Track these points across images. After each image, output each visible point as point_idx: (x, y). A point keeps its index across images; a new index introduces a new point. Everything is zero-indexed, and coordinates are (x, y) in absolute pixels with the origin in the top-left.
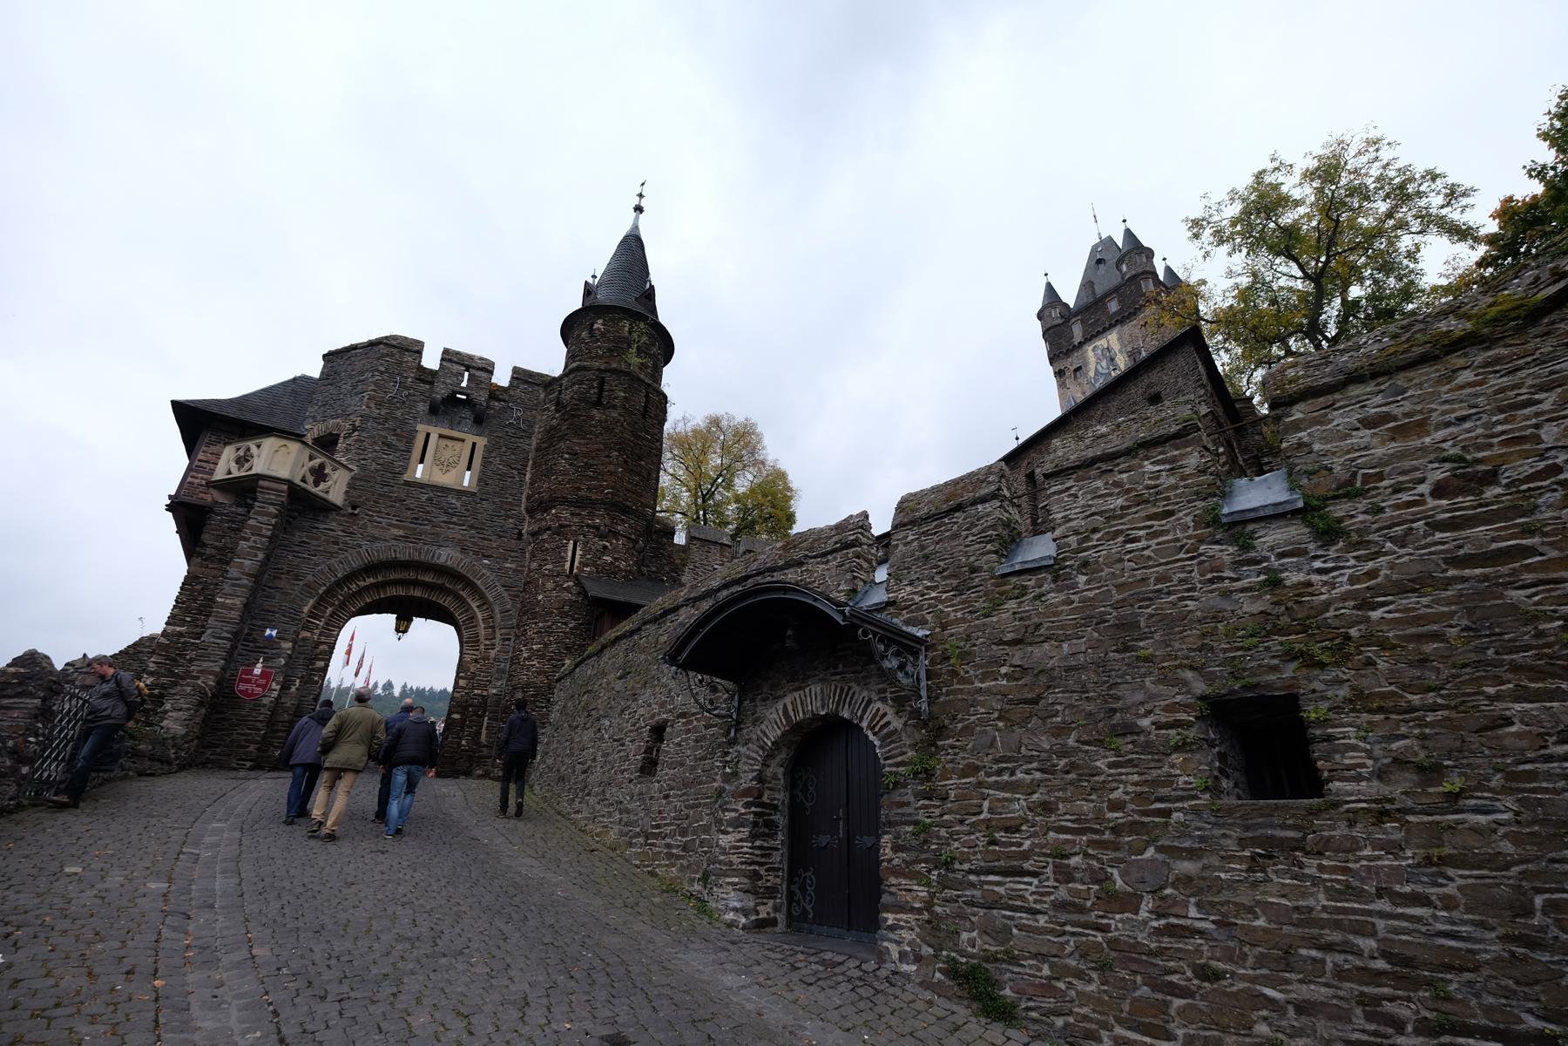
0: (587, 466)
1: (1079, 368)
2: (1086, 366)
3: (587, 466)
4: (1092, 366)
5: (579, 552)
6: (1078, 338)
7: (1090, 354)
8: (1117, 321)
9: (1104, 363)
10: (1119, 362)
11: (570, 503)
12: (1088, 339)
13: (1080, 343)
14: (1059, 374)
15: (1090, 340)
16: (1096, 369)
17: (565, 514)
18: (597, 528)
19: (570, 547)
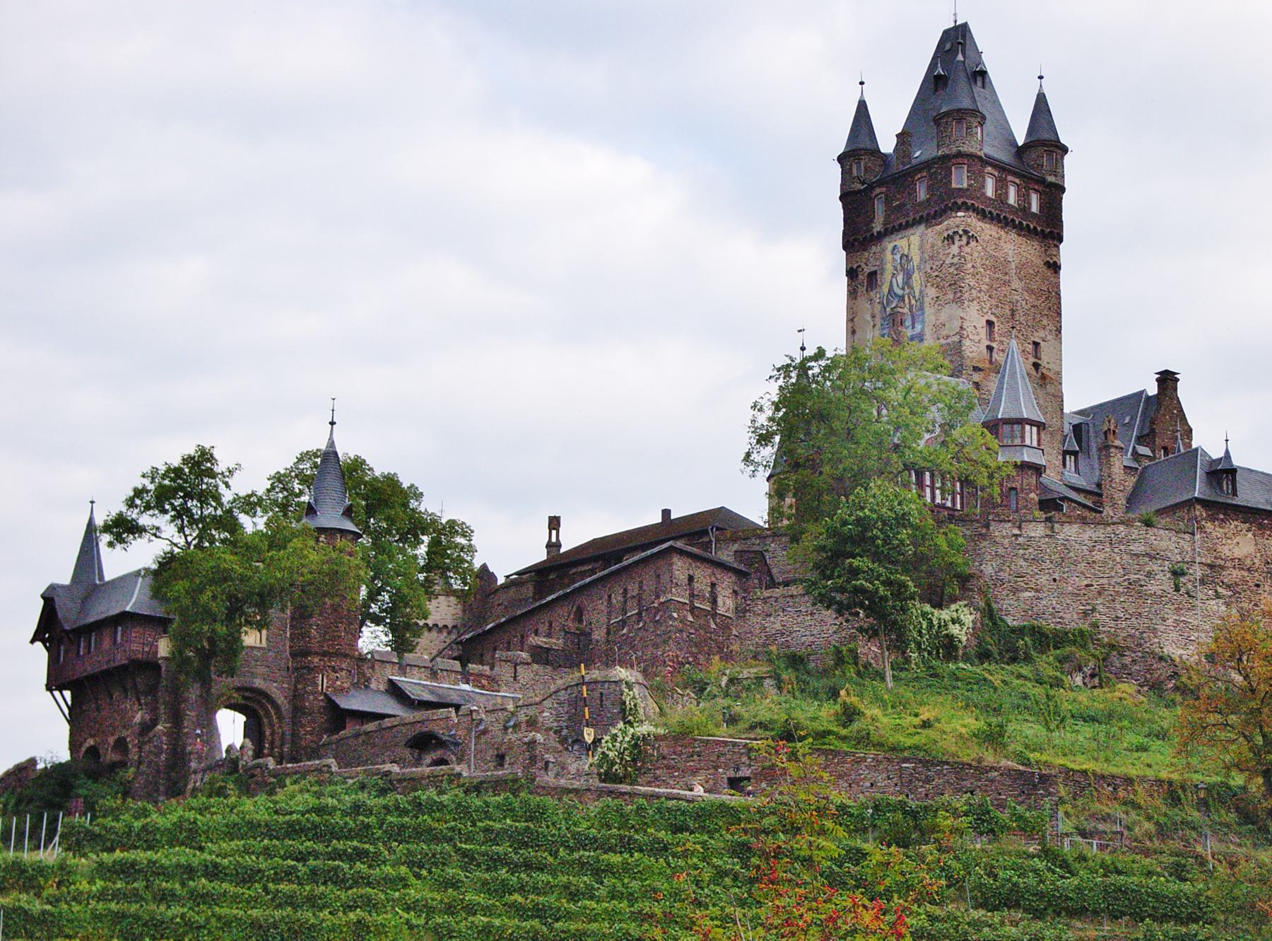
0: (326, 633)
1: (875, 272)
2: (882, 274)
3: (326, 633)
4: (887, 276)
5: (325, 681)
6: (878, 227)
7: (889, 257)
8: (922, 217)
9: (900, 278)
10: (914, 285)
11: (317, 654)
12: (889, 232)
13: (879, 233)
14: (852, 273)
15: (892, 233)
16: (891, 285)
17: (316, 660)
18: (334, 667)
19: (321, 679)
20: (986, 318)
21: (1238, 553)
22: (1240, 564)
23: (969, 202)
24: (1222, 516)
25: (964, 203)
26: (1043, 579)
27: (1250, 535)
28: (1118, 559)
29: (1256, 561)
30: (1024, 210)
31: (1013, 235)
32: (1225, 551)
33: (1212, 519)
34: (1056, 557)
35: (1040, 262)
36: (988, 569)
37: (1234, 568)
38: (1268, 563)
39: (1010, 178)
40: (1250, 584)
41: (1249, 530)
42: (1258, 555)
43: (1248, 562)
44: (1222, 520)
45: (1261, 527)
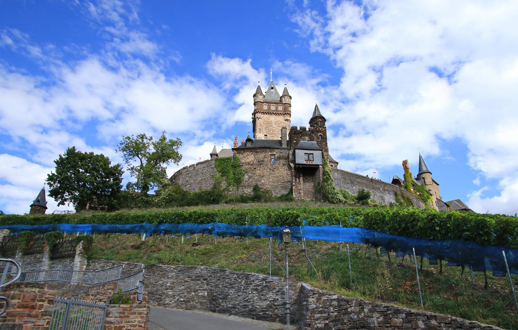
20: (264, 134)
21: (248, 161)
22: (249, 164)
23: (257, 111)
24: (242, 152)
25: (256, 112)
26: (192, 181)
27: (252, 155)
28: (209, 170)
29: (255, 162)
30: (277, 110)
31: (274, 116)
32: (243, 161)
33: (239, 153)
34: (195, 174)
35: (283, 121)
36: (180, 182)
37: (246, 165)
38: (259, 162)
39: (272, 104)
40: (252, 168)
41: (252, 154)
42: (256, 160)
43: (252, 163)
44: (243, 153)
45: (257, 152)
